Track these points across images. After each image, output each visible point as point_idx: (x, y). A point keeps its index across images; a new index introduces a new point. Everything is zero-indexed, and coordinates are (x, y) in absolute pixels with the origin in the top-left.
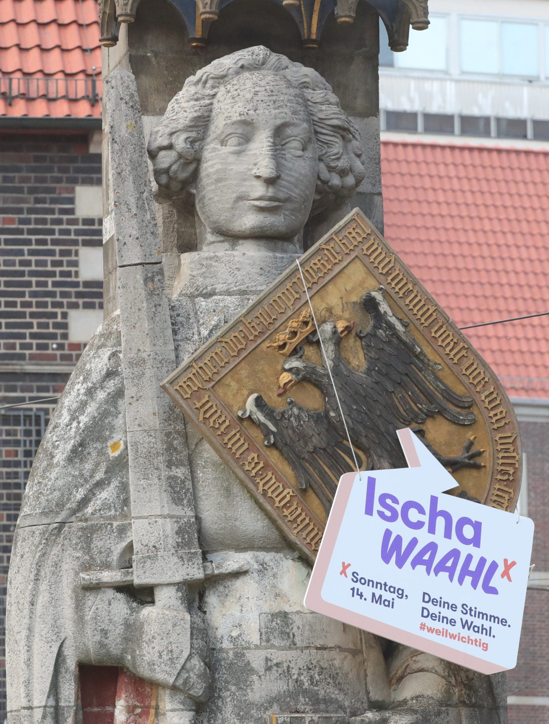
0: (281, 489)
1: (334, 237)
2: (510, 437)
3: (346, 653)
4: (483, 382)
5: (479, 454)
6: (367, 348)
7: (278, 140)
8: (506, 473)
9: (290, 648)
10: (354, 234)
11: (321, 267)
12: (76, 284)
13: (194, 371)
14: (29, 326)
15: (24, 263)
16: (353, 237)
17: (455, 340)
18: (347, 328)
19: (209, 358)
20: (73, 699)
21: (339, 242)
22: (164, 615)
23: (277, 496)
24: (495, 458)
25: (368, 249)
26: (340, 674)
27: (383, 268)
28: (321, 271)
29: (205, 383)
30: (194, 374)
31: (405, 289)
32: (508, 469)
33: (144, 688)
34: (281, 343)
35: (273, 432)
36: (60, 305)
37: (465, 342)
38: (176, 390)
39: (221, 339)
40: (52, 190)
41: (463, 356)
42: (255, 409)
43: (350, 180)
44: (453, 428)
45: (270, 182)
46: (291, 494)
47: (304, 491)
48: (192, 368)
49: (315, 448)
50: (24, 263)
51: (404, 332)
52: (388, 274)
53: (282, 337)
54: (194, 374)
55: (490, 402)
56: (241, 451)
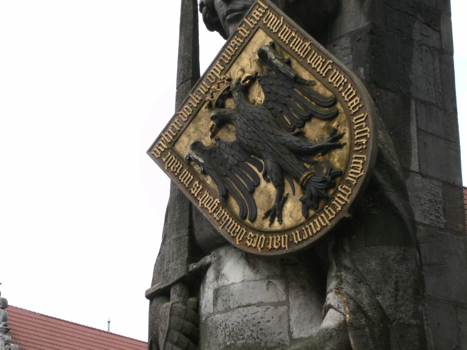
3: (268, 306)
4: (343, 83)
5: (341, 136)
8: (361, 144)
9: (226, 311)
17: (324, 60)
18: (247, 78)
19: (171, 128)
23: (209, 206)
24: (352, 135)
26: (262, 322)
27: (275, 29)
31: (290, 37)
32: (362, 140)
41: (329, 69)
44: (323, 124)
46: (219, 202)
49: (231, 166)
55: (348, 96)
56: (188, 183)
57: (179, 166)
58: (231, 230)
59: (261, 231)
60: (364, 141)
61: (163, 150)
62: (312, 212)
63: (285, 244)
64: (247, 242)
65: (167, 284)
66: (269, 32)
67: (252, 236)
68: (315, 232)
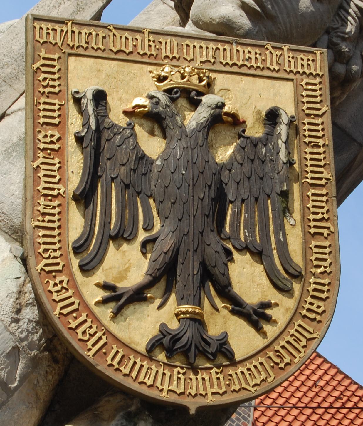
0: (56, 180)
1: (285, 49)
2: (311, 333)
10: (305, 63)
11: (253, 59)
13: (65, 29)
16: (302, 65)
21: (286, 56)
23: (46, 182)
25: (307, 84)
28: (251, 63)
29: (65, 45)
30: (62, 31)
34: (163, 74)
35: (89, 128)
37: (334, 225)
38: (35, 27)
39: (111, 28)
42: (90, 96)
46: (61, 192)
48: (64, 25)
51: (284, 163)
54: (62, 31)
55: (315, 290)
57: (54, 87)
58: (44, 243)
61: (51, 39)
63: (94, 345)
64: (52, 283)
67: (64, 284)
68: (141, 379)
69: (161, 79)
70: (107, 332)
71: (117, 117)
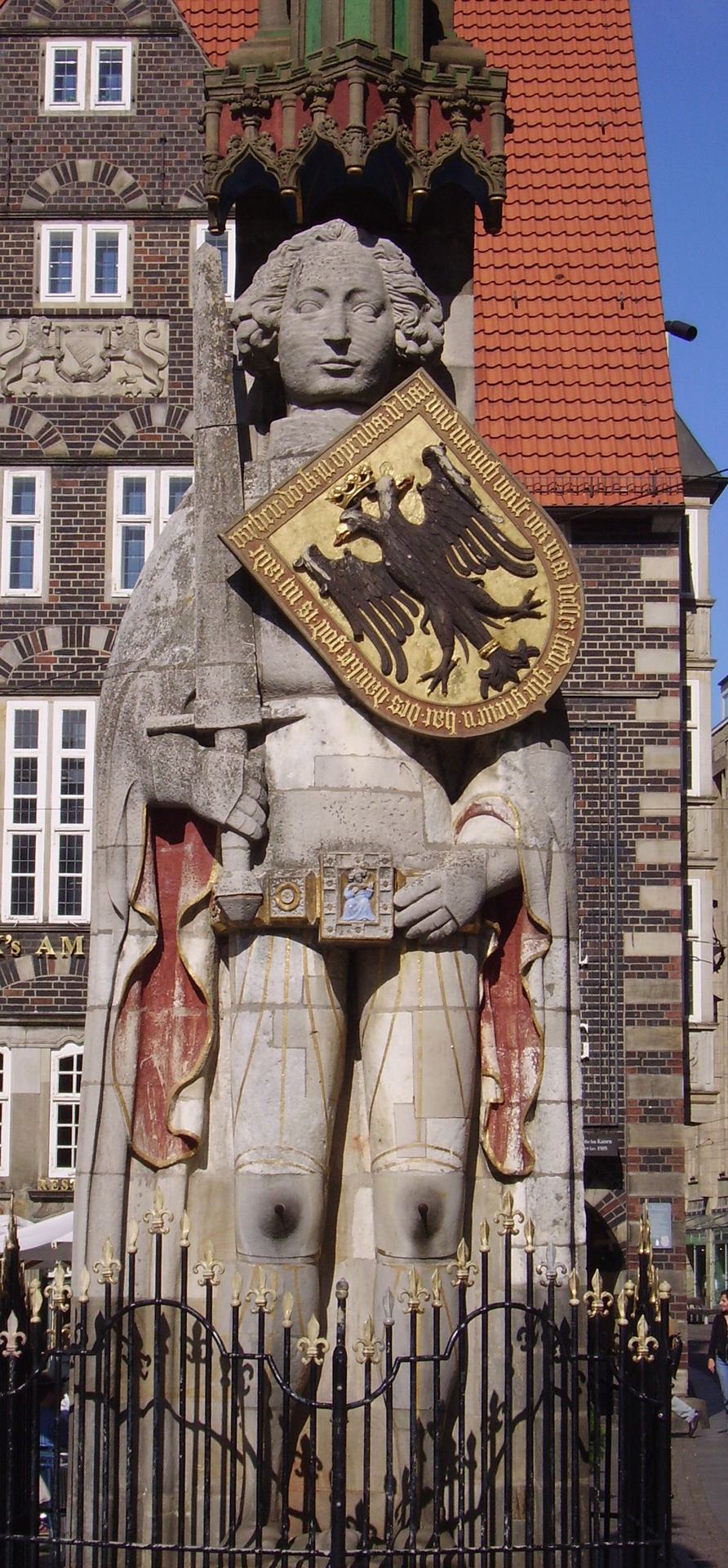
5: (539, 604)
6: (426, 501)
7: (349, 306)
8: (568, 623)
12: (641, 630)
14: (607, 661)
15: (601, 615)
20: (142, 836)
22: (225, 756)
33: (211, 832)
36: (629, 646)
40: (624, 561)
42: (307, 558)
43: (428, 347)
44: (515, 579)
45: (341, 346)
47: (359, 638)
50: (601, 615)
52: (450, 431)
53: (340, 486)
59: (414, 699)
60: (572, 620)
62: (492, 693)
65: (215, 726)
66: (434, 427)
69: (339, 500)
70: (452, 708)
71: (336, 554)
